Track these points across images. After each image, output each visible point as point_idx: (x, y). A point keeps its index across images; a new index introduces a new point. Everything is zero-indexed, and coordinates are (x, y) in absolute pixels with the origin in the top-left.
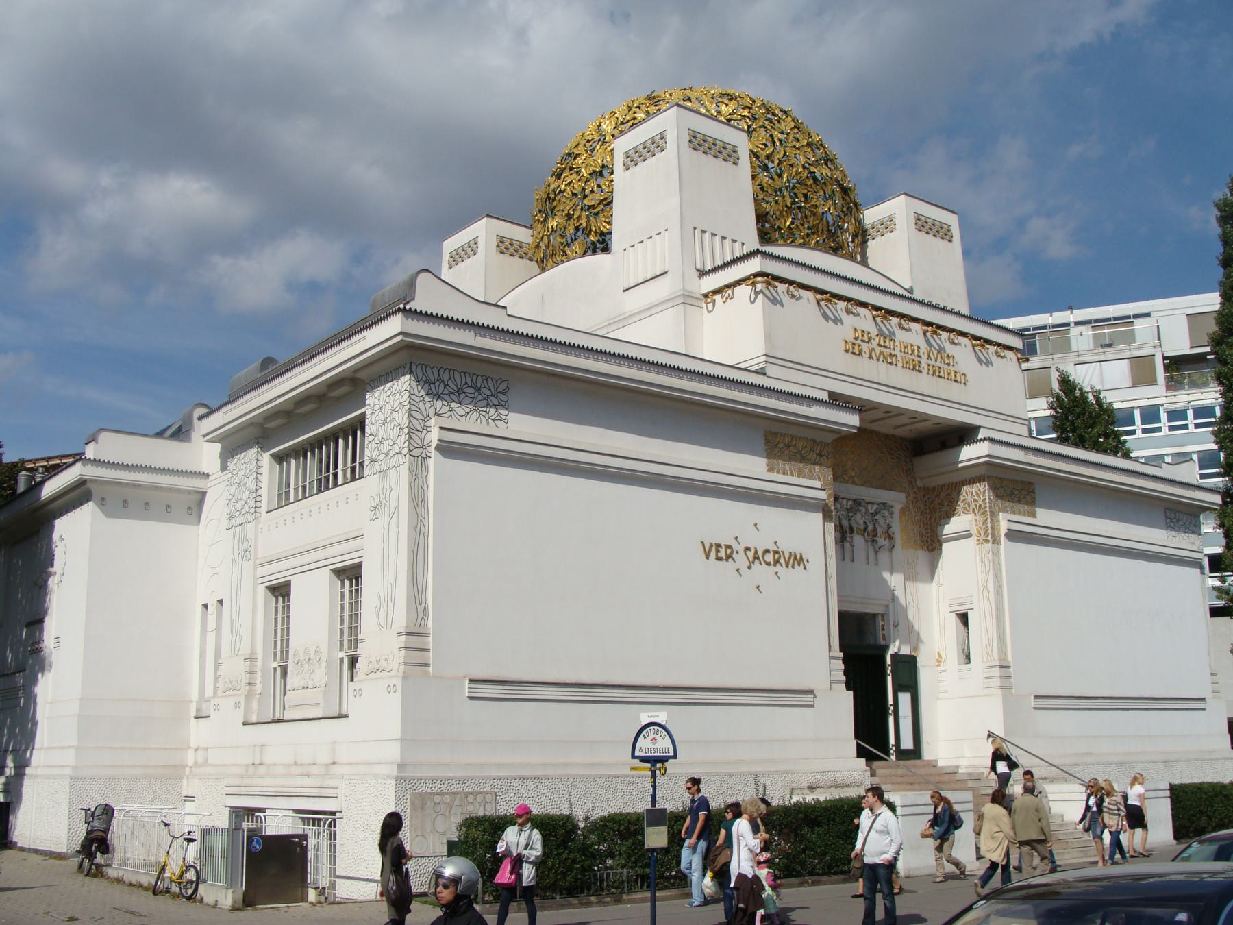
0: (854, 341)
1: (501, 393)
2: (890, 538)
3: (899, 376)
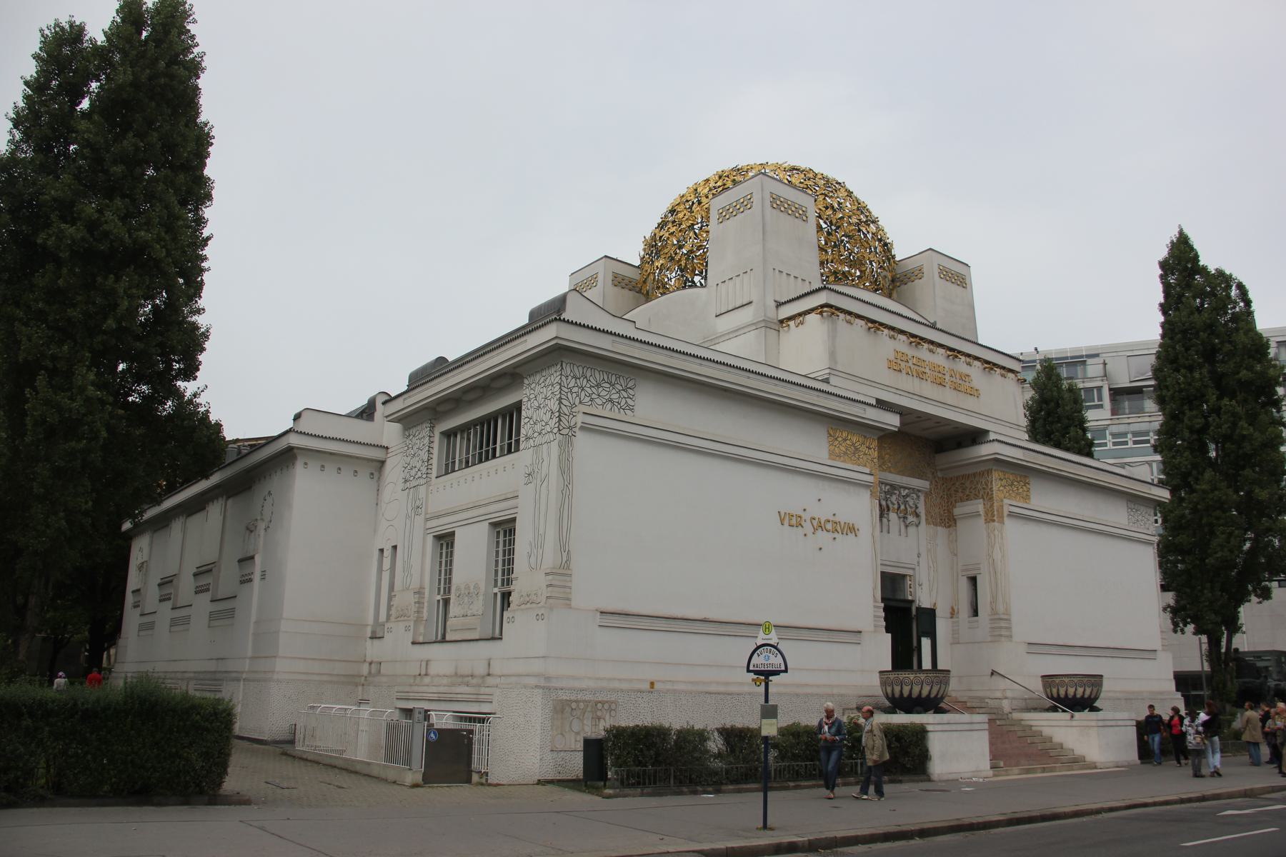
1: (629, 388)
2: (917, 516)
3: (928, 389)
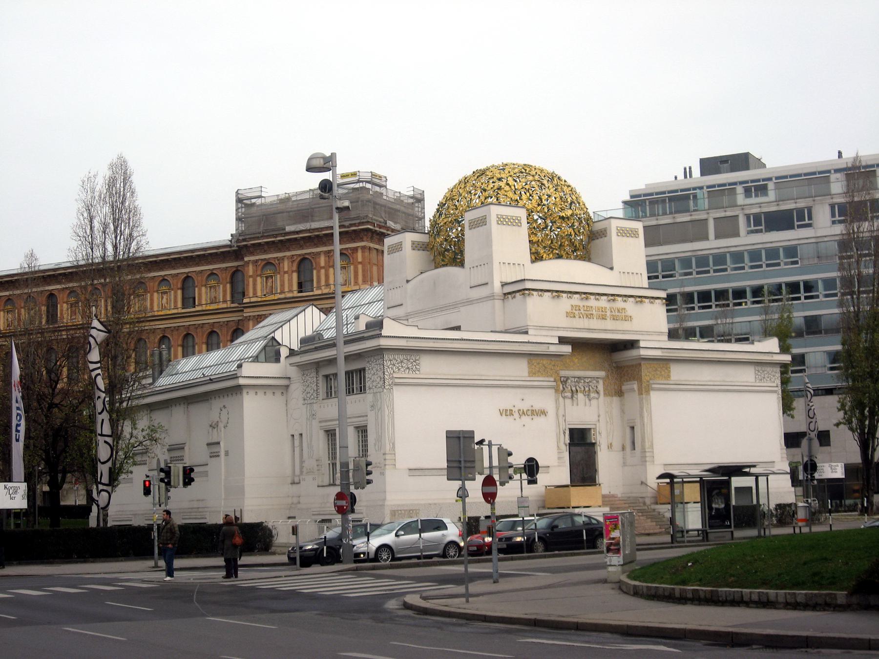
3: (594, 323)
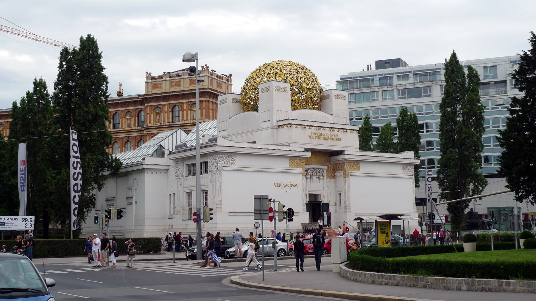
0: (311, 135)
3: (323, 142)
